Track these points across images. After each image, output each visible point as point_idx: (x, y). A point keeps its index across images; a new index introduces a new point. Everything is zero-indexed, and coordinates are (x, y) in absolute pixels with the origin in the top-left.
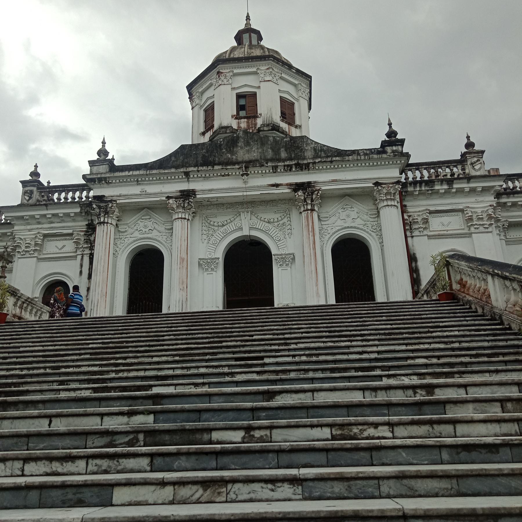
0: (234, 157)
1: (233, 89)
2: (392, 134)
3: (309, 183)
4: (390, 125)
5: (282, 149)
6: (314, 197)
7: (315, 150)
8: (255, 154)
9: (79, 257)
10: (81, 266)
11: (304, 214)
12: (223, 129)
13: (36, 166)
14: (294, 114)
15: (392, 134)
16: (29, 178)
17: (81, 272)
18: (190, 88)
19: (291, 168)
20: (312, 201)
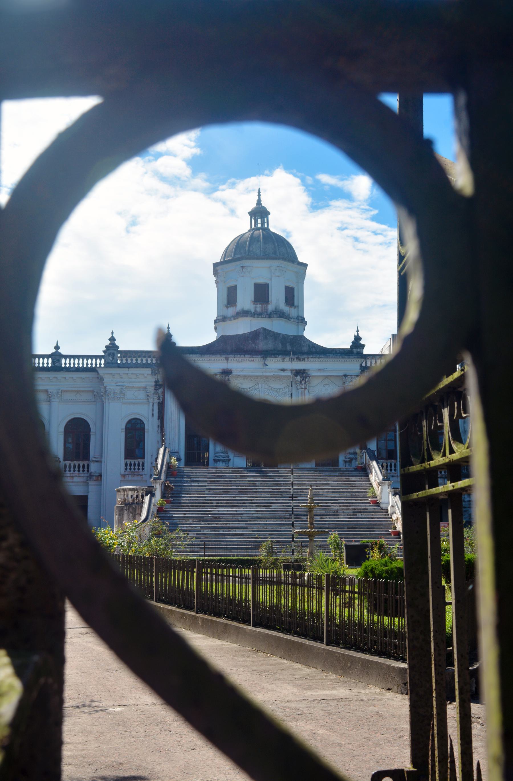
0: (257, 347)
1: (253, 279)
2: (358, 338)
3: (304, 370)
4: (358, 331)
5: (288, 344)
6: (307, 380)
7: (309, 346)
8: (269, 346)
9: (151, 404)
10: (153, 410)
11: (300, 391)
12: (245, 313)
13: (112, 333)
14: (294, 296)
15: (358, 338)
16: (108, 343)
17: (153, 415)
18: (215, 265)
19: (294, 359)
20: (305, 383)
